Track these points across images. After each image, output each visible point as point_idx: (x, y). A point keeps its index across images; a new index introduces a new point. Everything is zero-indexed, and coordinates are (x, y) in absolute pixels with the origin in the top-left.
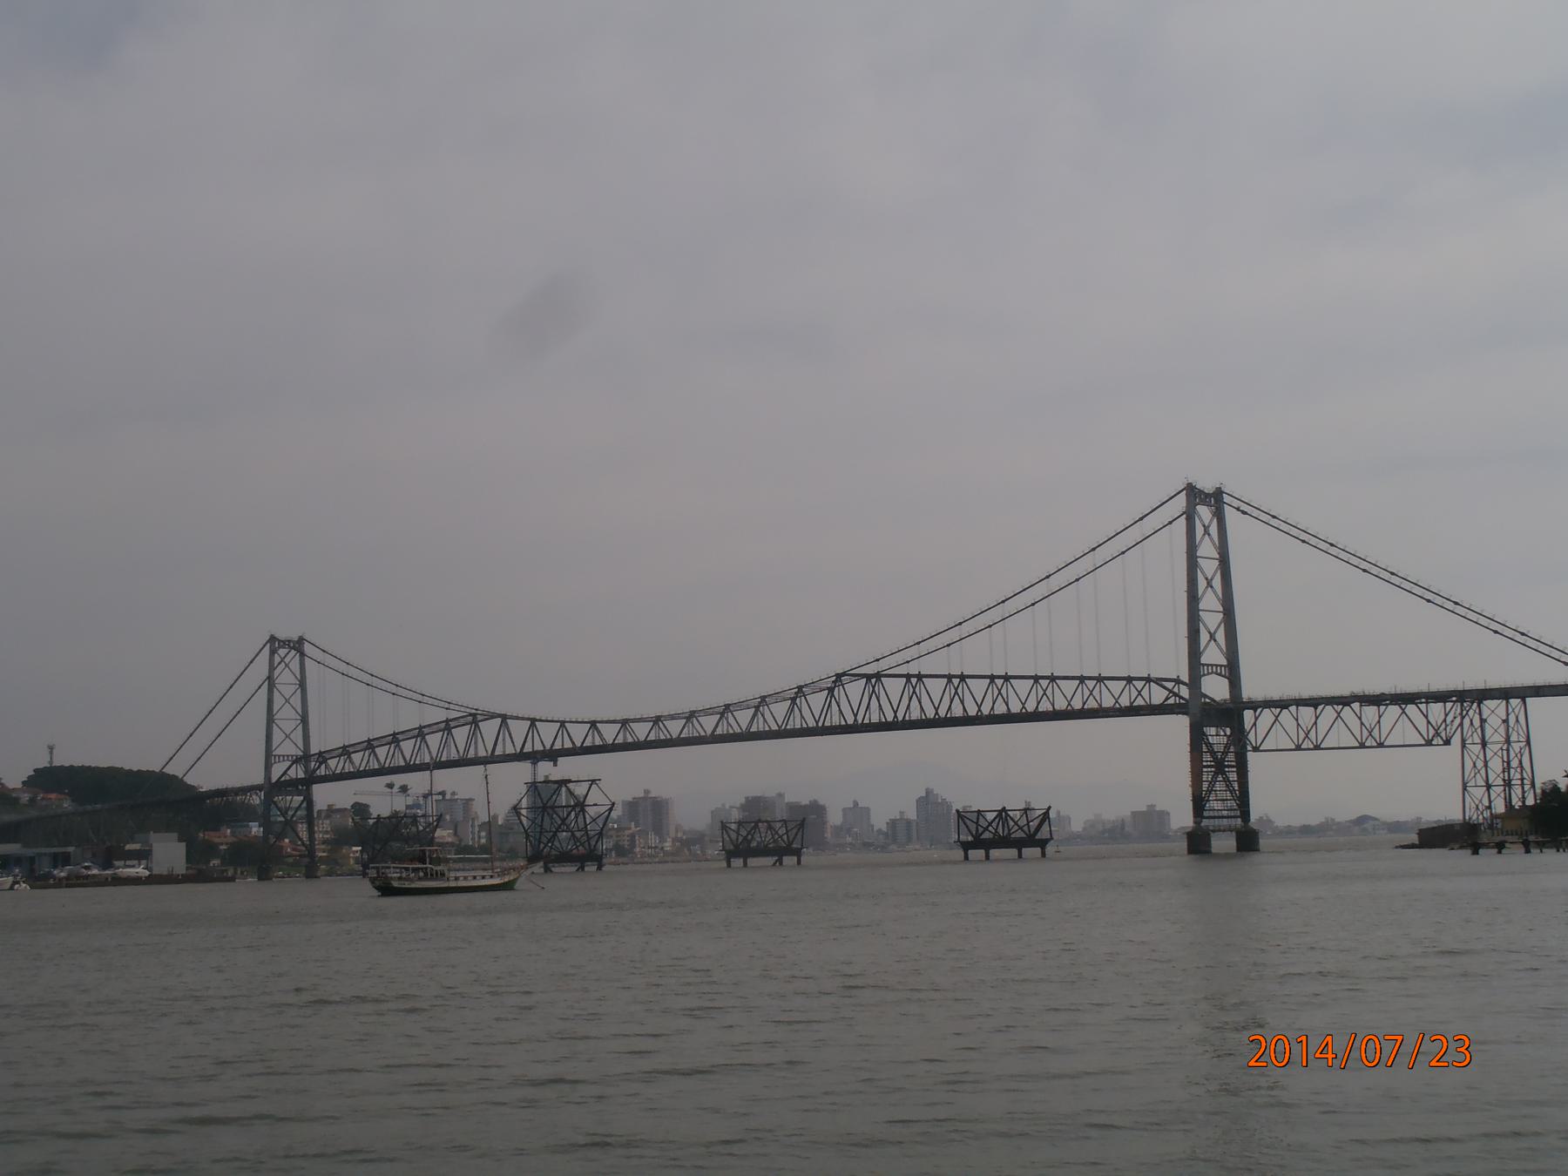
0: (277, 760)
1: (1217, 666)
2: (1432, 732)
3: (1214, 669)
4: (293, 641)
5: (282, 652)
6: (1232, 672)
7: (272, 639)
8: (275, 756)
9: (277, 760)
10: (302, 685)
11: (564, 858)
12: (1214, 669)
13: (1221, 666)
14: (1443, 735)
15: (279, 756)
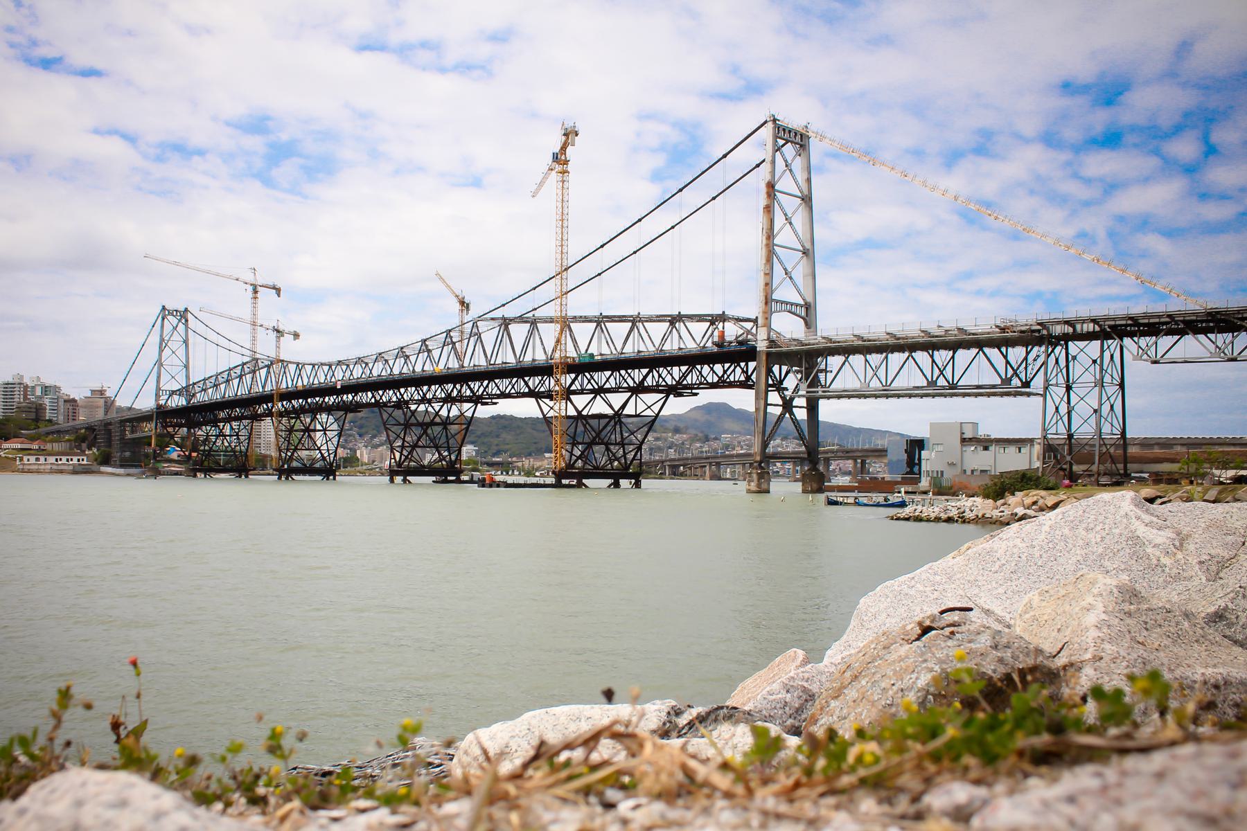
0: (164, 394)
1: (792, 304)
2: (1010, 372)
3: (789, 307)
4: (180, 312)
5: (174, 320)
6: (808, 312)
7: (164, 308)
8: (163, 391)
9: (164, 394)
10: (186, 342)
11: (308, 470)
12: (789, 307)
13: (797, 305)
14: (1023, 376)
15: (166, 391)
